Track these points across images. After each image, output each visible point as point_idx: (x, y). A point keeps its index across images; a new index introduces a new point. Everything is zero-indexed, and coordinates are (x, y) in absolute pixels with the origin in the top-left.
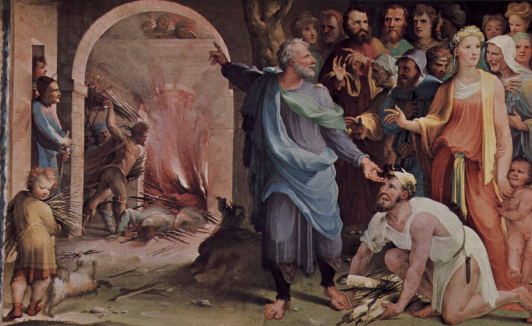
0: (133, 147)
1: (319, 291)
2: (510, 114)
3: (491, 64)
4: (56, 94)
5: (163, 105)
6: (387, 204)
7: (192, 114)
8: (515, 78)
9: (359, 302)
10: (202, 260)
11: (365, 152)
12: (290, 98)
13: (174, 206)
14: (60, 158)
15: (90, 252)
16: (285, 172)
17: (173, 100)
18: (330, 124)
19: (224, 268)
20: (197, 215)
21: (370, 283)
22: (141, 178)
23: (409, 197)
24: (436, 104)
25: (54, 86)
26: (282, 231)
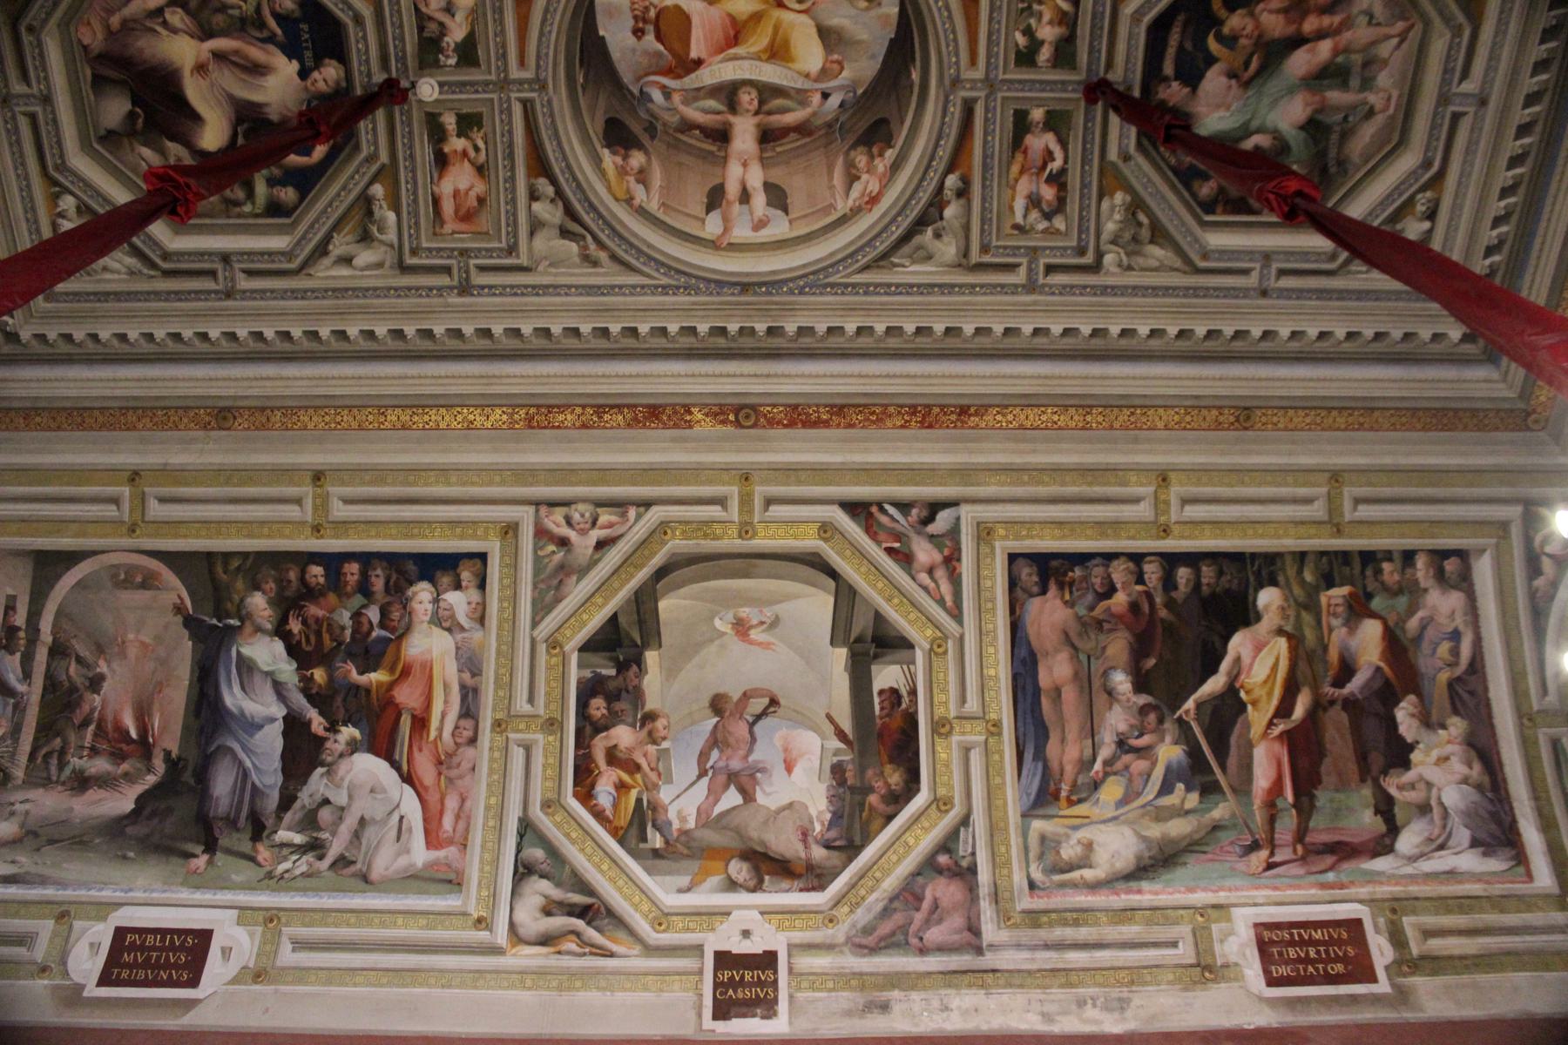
0: (88, 696)
1: (246, 846)
2: (460, 671)
3: (443, 620)
4: (22, 642)
5: (123, 654)
6: (329, 759)
7: (150, 666)
8: (465, 635)
9: (285, 859)
10: (136, 812)
11: (314, 706)
12: (246, 651)
13: (118, 757)
14: (16, 706)
15: (27, 801)
16: (234, 726)
17: (132, 652)
18: (282, 678)
19: (156, 821)
20: (139, 765)
21: (298, 839)
22: (92, 727)
23: (352, 753)
24: (388, 658)
25: (22, 634)
26: (222, 785)
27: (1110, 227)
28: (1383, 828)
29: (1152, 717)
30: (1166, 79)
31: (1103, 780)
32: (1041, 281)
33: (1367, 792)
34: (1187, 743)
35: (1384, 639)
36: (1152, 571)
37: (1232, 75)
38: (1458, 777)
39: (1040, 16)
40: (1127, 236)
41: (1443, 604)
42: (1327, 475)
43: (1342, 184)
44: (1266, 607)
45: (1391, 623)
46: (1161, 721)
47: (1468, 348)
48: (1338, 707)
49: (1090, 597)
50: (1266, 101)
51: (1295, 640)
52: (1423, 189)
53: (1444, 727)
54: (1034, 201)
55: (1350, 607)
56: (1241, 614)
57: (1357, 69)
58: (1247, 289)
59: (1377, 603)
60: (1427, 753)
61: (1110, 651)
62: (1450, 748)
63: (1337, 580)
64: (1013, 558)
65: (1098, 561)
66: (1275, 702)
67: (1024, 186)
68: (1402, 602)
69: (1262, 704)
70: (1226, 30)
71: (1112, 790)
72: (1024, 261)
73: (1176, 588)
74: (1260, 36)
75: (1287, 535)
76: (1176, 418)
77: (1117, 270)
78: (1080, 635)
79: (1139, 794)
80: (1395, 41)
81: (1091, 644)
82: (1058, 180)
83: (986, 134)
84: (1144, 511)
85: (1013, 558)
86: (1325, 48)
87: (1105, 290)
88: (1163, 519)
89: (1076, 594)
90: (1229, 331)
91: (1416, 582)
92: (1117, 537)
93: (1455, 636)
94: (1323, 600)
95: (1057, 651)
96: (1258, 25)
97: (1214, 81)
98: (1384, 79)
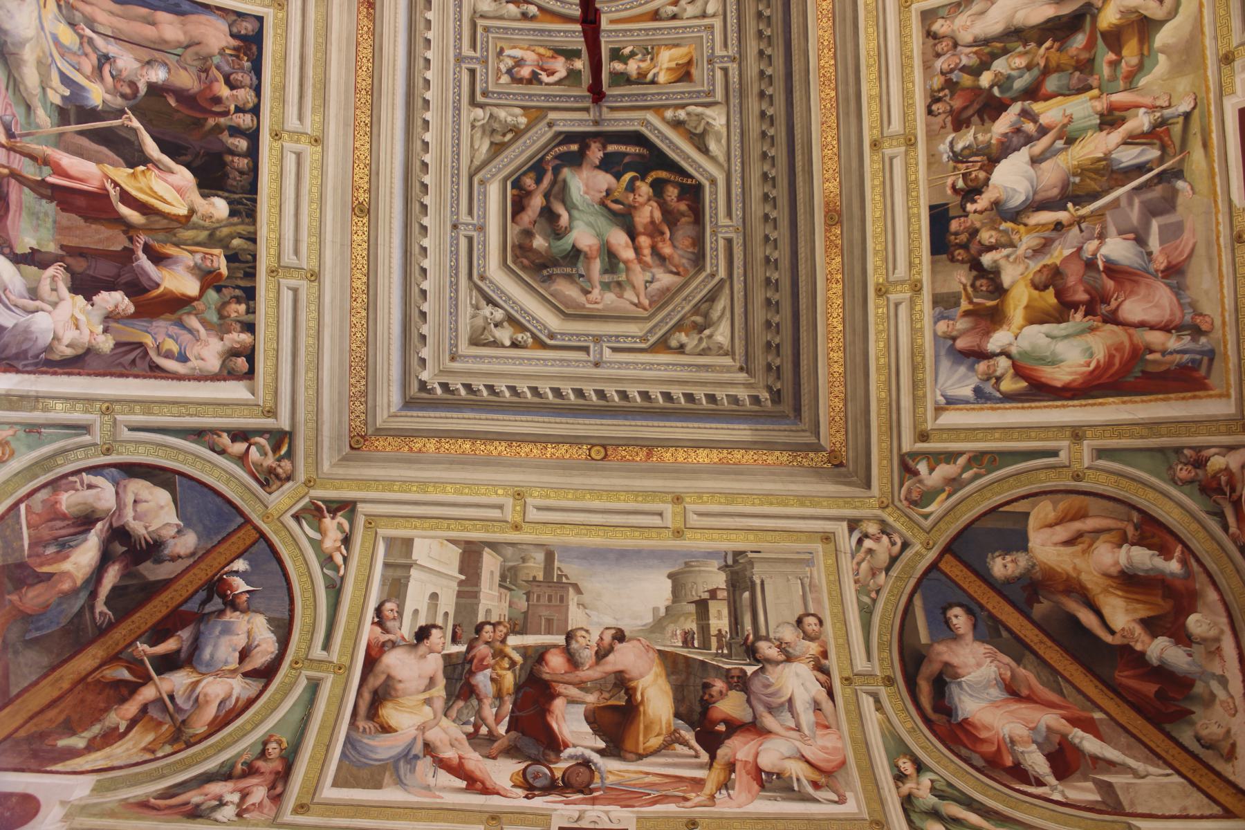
27: (502, 114)
28: (19, 251)
29: (127, 90)
30: (604, 147)
31: (78, 34)
32: (464, 66)
33: (52, 248)
34: (103, 111)
35: (183, 295)
36: (245, 120)
37: (609, 192)
38: (60, 333)
39: (643, 61)
40: (496, 126)
41: (210, 353)
42: (317, 269)
43: (535, 280)
44: (213, 204)
45: (195, 303)
46: (123, 96)
47: (415, 386)
48: (127, 244)
49: (227, 69)
50: (592, 219)
51: (185, 221)
52: (534, 336)
53: (105, 331)
54: (519, 63)
55: (210, 272)
56: (211, 176)
57: (615, 278)
58: (457, 214)
59: (212, 295)
60: (83, 311)
61: (182, 72)
62: (86, 332)
63: (232, 265)
64: (260, 19)
65: (255, 81)
66: (134, 193)
67: (530, 57)
68: (213, 317)
69: (133, 181)
70: (638, 183)
71: (67, 36)
72: (478, 55)
73: (231, 136)
74: (635, 208)
75: (270, 230)
76: (362, 157)
77: (472, 118)
78: (197, 54)
79: (62, 56)
80: (636, 301)
81: (189, 61)
82: (534, 79)
83: (565, 32)
84: (292, 123)
85: (260, 19)
86: (628, 254)
87: (457, 109)
88: (285, 136)
89: (230, 59)
90: (427, 200)
91: (229, 332)
92: (273, 99)
93: (183, 358)
94: (217, 251)
95: (185, 33)
96: (643, 205)
97: (604, 180)
98: (610, 297)
